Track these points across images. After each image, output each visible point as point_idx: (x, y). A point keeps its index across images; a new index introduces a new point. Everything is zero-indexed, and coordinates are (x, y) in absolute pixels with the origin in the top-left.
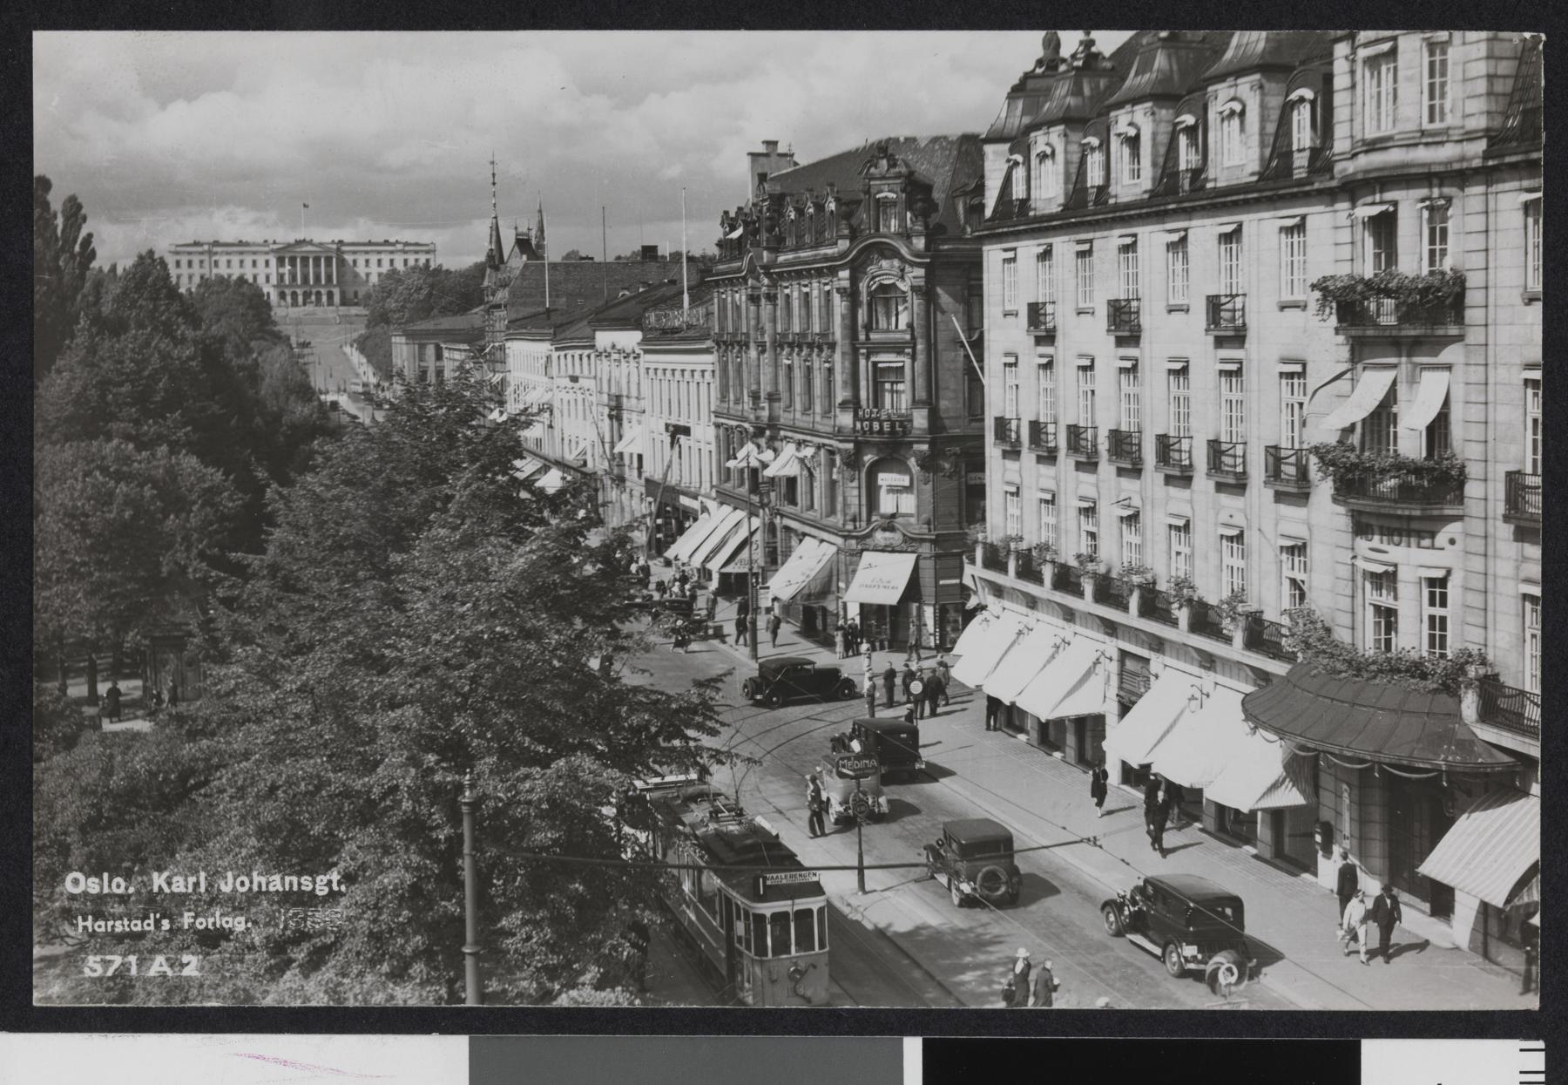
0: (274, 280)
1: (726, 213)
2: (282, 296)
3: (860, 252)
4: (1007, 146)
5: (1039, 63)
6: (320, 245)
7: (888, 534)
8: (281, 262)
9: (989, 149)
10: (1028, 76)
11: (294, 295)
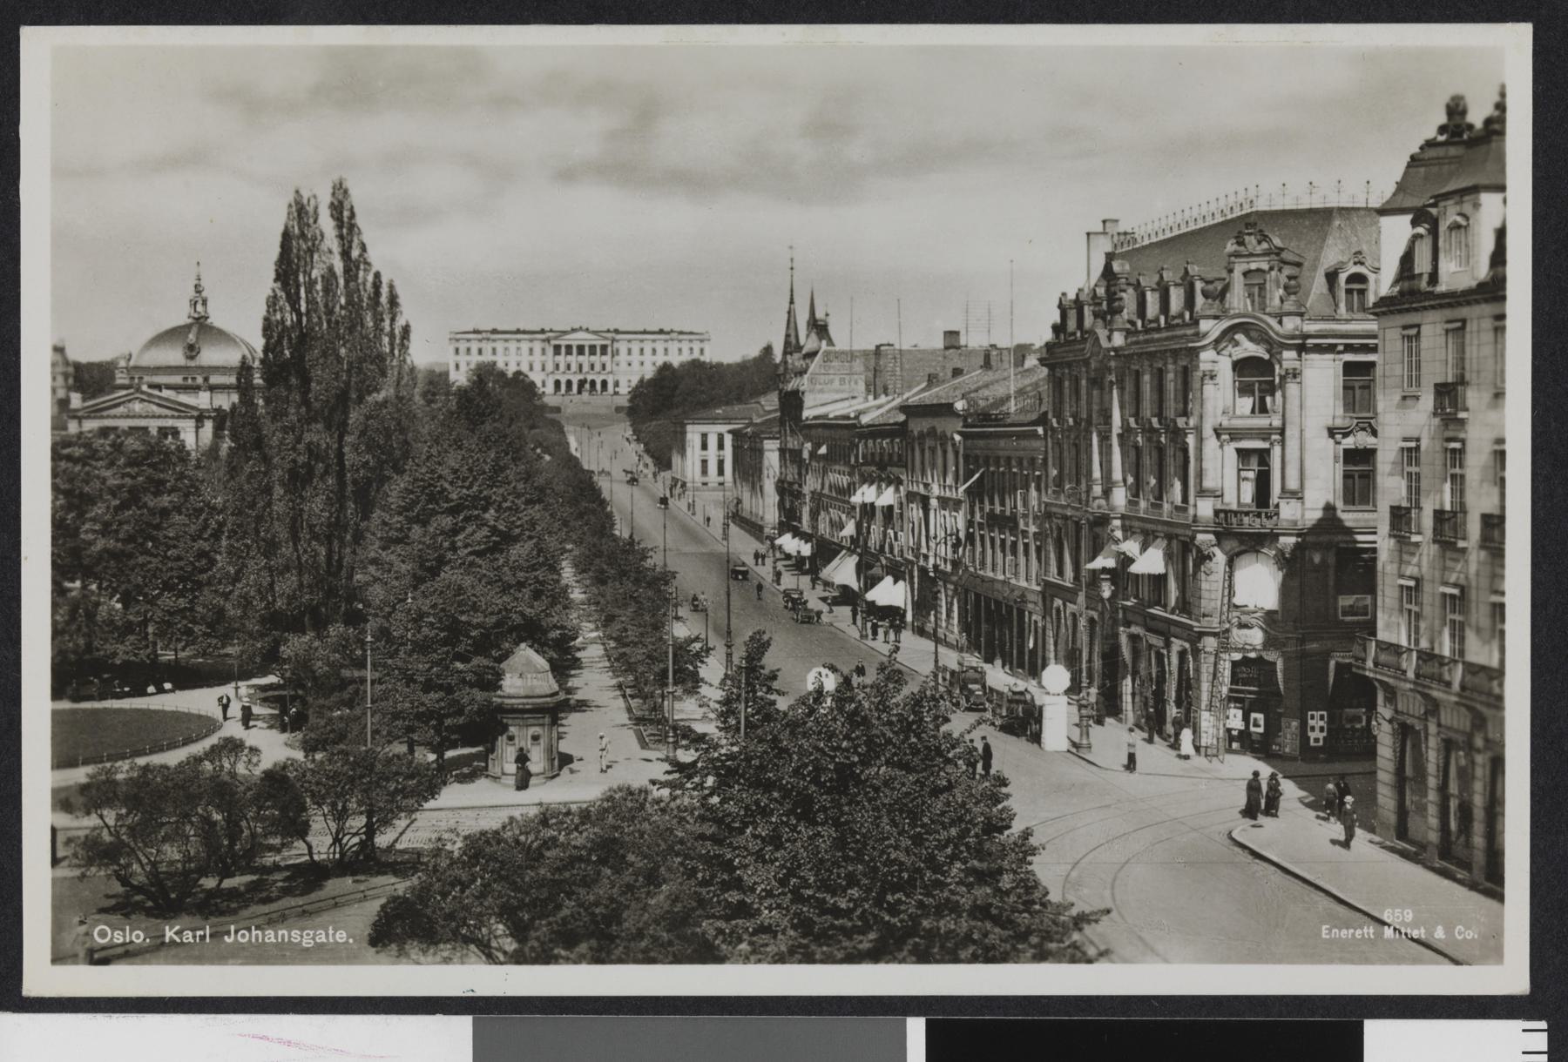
0: (550, 367)
1: (1064, 294)
2: (557, 384)
3: (1225, 333)
4: (1409, 217)
5: (1442, 129)
6: (595, 332)
7: (1245, 631)
8: (557, 349)
9: (1386, 222)
10: (1430, 144)
11: (569, 383)
